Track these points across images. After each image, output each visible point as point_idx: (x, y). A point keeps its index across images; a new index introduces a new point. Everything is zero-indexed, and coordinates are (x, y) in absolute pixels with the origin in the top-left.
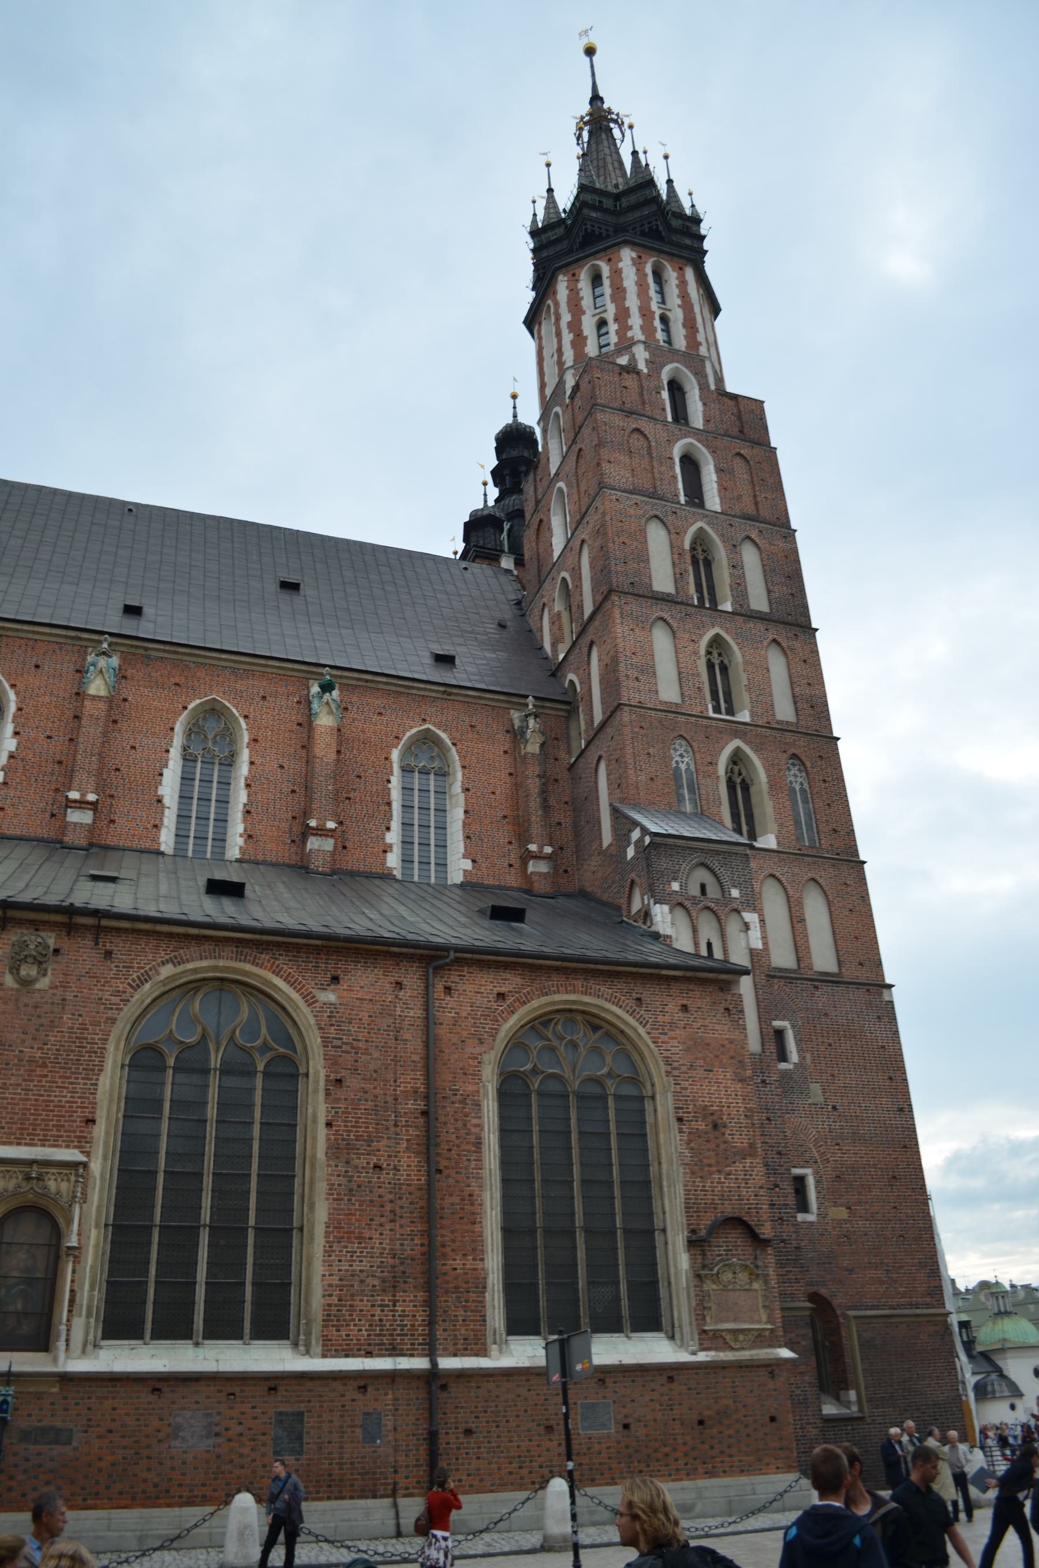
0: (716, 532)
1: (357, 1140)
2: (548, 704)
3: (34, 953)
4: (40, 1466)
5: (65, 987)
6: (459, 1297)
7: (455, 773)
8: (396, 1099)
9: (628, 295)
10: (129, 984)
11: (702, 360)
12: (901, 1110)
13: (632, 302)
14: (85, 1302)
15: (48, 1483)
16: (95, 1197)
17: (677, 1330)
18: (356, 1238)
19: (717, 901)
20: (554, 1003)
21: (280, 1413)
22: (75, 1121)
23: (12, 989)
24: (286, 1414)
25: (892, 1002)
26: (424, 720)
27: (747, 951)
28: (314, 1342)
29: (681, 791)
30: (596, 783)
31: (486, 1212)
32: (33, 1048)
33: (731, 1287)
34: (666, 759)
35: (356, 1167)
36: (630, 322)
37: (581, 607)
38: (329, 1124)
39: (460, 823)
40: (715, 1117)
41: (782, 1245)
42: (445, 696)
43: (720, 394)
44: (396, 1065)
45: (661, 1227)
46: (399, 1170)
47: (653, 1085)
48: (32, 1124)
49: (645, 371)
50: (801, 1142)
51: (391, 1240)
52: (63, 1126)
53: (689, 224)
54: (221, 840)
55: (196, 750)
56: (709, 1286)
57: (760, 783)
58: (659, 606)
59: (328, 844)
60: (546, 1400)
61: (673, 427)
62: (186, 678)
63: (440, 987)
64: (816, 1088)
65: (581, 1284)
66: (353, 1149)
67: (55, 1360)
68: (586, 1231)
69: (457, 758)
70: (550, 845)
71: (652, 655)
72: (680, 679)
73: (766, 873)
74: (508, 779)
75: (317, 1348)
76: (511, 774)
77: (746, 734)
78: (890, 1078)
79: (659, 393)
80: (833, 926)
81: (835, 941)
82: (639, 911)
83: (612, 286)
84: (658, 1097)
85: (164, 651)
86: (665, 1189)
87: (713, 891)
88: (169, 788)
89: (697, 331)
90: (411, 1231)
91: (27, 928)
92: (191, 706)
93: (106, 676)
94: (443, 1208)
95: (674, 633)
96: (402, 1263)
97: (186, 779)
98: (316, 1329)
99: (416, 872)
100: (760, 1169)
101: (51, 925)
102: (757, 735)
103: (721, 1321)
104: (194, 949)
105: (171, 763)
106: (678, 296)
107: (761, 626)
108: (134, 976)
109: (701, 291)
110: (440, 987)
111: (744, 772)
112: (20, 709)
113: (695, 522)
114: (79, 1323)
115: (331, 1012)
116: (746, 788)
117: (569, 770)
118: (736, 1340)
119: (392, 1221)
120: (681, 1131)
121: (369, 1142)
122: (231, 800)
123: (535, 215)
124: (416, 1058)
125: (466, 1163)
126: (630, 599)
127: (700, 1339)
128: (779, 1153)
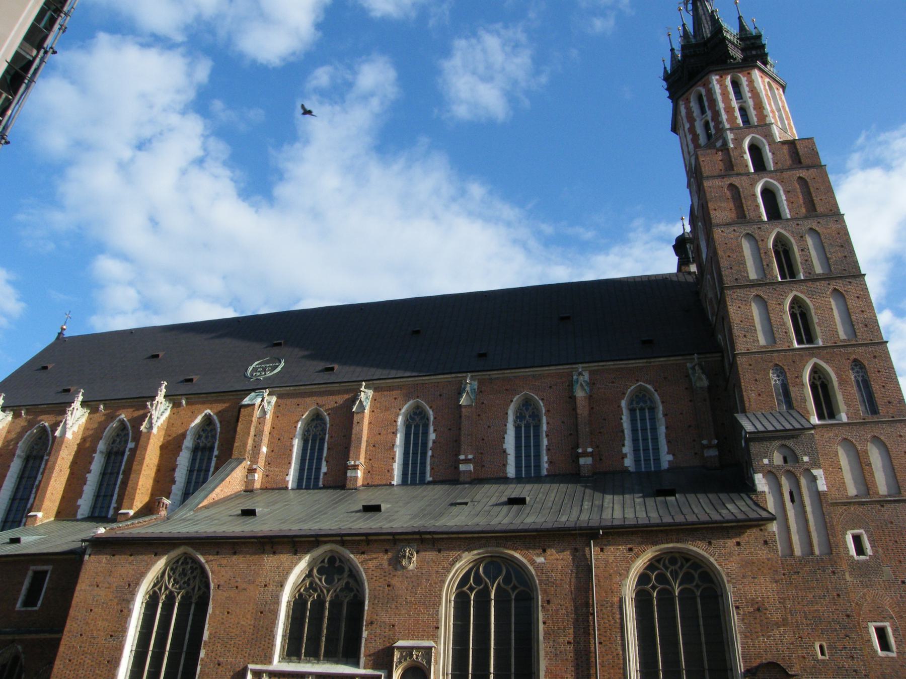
26: (638, 381)
54: (538, 466)
69: (658, 398)
76: (691, 401)
79: (743, 157)
92: (515, 399)
99: (643, 466)
111: (822, 376)
123: (665, 68)
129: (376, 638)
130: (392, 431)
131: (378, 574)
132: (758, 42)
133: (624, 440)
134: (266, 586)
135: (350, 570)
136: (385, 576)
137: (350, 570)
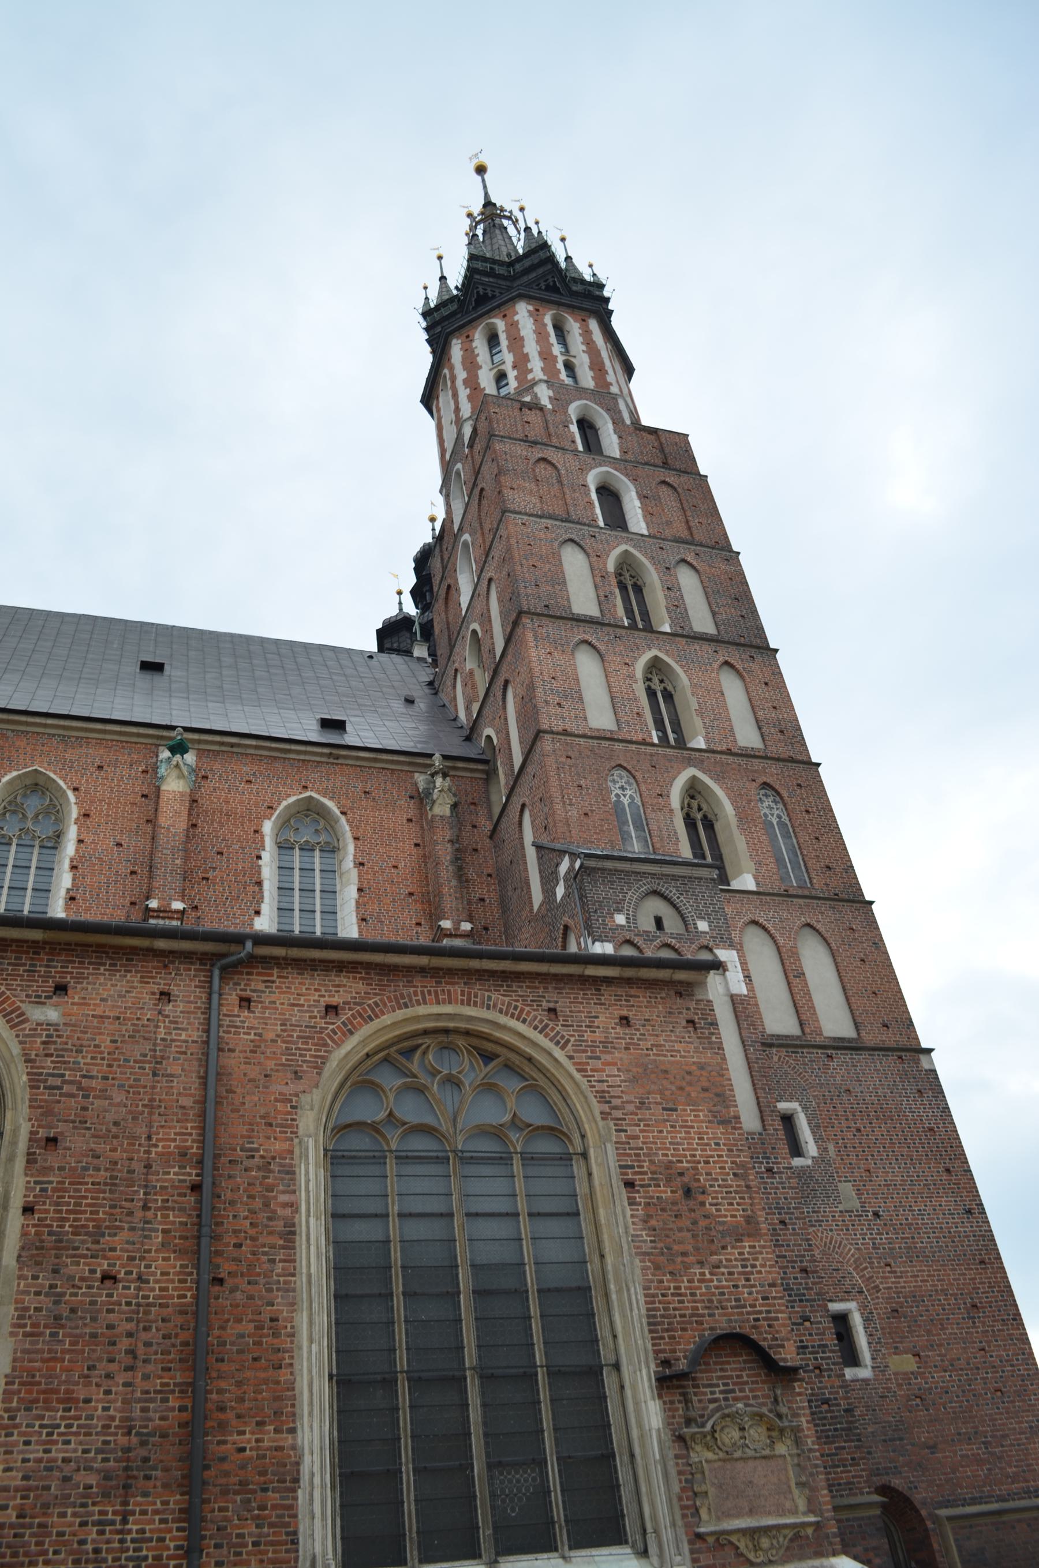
0: (645, 555)
1: (74, 1234)
2: (460, 764)
6: (249, 1501)
7: (346, 846)
8: (148, 1166)
9: (526, 343)
11: (614, 398)
12: (969, 1212)
13: (531, 347)
17: (651, 1538)
18: (59, 1401)
19: (679, 937)
20: (417, 1019)
25: (935, 1071)
26: (305, 787)
27: (728, 999)
29: (625, 828)
31: (300, 1348)
33: (738, 1454)
34: (603, 793)
35: (71, 1278)
38: (28, 1210)
39: (353, 903)
40: (686, 1179)
41: (825, 1407)
42: (331, 760)
43: (636, 429)
44: (151, 1114)
45: (613, 1361)
46: (147, 1282)
47: (583, 1136)
49: (550, 406)
50: (834, 1265)
53: (591, 288)
56: (700, 1454)
57: (726, 816)
61: (588, 458)
63: (232, 998)
64: (847, 1189)
65: (478, 1467)
66: (67, 1248)
68: (481, 1377)
69: (347, 828)
70: (470, 919)
73: (746, 919)
74: (414, 850)
76: (417, 845)
77: (702, 761)
78: (948, 1170)
80: (841, 980)
81: (847, 999)
83: (508, 338)
84: (592, 1152)
86: (614, 1297)
87: (672, 924)
90: (162, 1385)
94: (224, 1344)
96: (143, 1444)
100: (767, 1256)
102: (716, 762)
103: (729, 1515)
107: (707, 648)
109: (609, 346)
110: (232, 998)
111: (704, 806)
113: (618, 545)
116: (709, 825)
117: (491, 837)
118: (757, 1548)
119: (129, 1368)
120: (632, 1202)
121: (97, 1235)
124: (185, 1101)
125: (267, 1266)
126: (545, 621)
127: (692, 1552)
128: (804, 1270)
133: (261, 900)
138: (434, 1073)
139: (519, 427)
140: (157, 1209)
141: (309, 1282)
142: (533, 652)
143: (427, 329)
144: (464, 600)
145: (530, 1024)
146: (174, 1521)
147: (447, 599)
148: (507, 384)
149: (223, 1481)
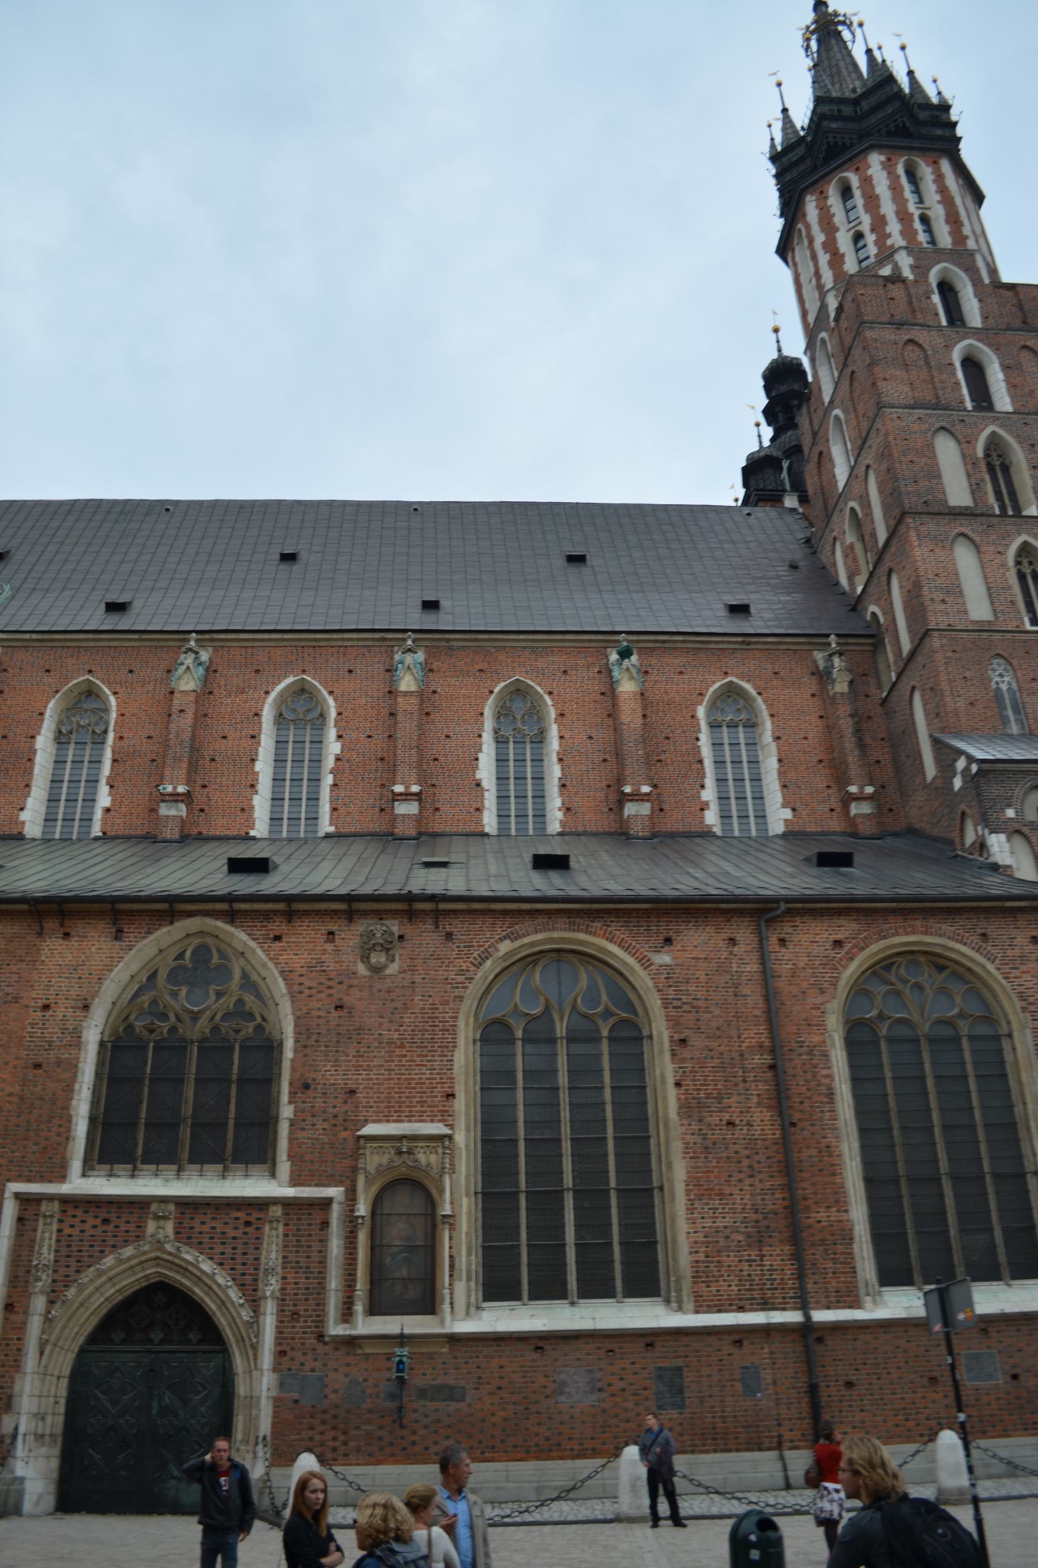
0: (1011, 433)
1: (708, 1098)
2: (851, 640)
3: (381, 941)
4: (438, 1421)
5: (413, 970)
7: (763, 723)
10: (471, 963)
11: (971, 254)
13: (888, 208)
14: (464, 1267)
15: (447, 1437)
16: (462, 1168)
20: (893, 946)
21: (660, 1369)
22: (436, 1097)
23: (365, 977)
24: (665, 1369)
26: (726, 673)
28: (685, 1299)
29: (1005, 713)
30: (912, 715)
32: (390, 1030)
34: (985, 681)
35: (709, 1125)
36: (888, 230)
37: (874, 535)
38: (678, 1084)
43: (996, 287)
46: (752, 1126)
47: (1009, 1023)
48: (396, 1102)
49: (911, 277)
51: (752, 1195)
52: (425, 1102)
53: (937, 113)
54: (541, 816)
55: (507, 732)
58: (958, 522)
59: (645, 808)
60: (927, 1351)
61: (949, 331)
62: (489, 663)
63: (774, 939)
65: (953, 1232)
67: (442, 1322)
69: (763, 707)
71: (957, 574)
72: (990, 596)
74: (819, 722)
75: (689, 1304)
76: (821, 717)
79: (929, 298)
82: (974, 843)
83: (864, 195)
84: (1016, 1035)
85: (465, 640)
88: (486, 770)
89: (961, 224)
91: (372, 918)
92: (497, 690)
93: (414, 671)
95: (977, 548)
96: (765, 1218)
97: (501, 761)
98: (687, 1285)
99: (736, 827)
101: (394, 914)
104: (528, 924)
105: (485, 747)
106: (937, 192)
108: (476, 955)
109: (961, 182)
110: (774, 939)
112: (340, 714)
113: (986, 427)
114: (460, 1287)
115: (668, 973)
119: (751, 1176)
121: (719, 1098)
122: (546, 776)
123: (772, 139)
126: (926, 518)
129: (315, 1119)
130: (252, 733)
131: (314, 984)
132: (944, 116)
133: (703, 776)
134: (46, 1007)
135: (245, 976)
136: (329, 988)
137: (245, 976)
138: (905, 982)
139: (886, 307)
140: (753, 1081)
141: (846, 1125)
142: (917, 552)
143: (777, 176)
144: (841, 474)
145: (969, 947)
146: (789, 1260)
147: (819, 463)
148: (865, 246)
149: (811, 1239)
